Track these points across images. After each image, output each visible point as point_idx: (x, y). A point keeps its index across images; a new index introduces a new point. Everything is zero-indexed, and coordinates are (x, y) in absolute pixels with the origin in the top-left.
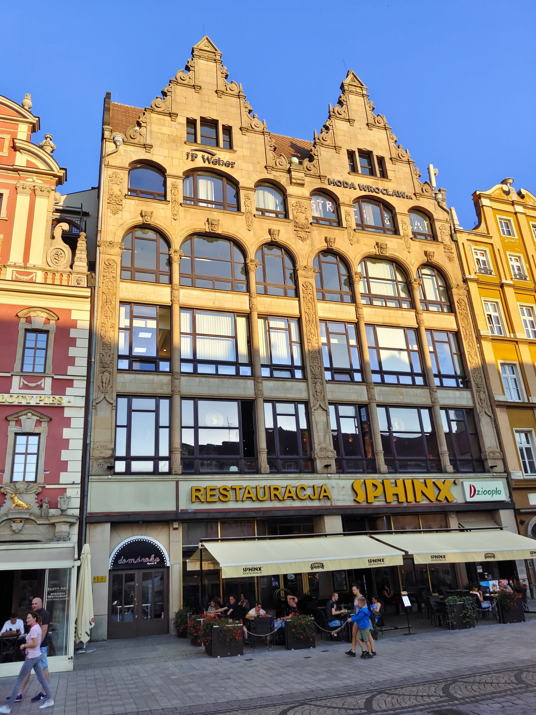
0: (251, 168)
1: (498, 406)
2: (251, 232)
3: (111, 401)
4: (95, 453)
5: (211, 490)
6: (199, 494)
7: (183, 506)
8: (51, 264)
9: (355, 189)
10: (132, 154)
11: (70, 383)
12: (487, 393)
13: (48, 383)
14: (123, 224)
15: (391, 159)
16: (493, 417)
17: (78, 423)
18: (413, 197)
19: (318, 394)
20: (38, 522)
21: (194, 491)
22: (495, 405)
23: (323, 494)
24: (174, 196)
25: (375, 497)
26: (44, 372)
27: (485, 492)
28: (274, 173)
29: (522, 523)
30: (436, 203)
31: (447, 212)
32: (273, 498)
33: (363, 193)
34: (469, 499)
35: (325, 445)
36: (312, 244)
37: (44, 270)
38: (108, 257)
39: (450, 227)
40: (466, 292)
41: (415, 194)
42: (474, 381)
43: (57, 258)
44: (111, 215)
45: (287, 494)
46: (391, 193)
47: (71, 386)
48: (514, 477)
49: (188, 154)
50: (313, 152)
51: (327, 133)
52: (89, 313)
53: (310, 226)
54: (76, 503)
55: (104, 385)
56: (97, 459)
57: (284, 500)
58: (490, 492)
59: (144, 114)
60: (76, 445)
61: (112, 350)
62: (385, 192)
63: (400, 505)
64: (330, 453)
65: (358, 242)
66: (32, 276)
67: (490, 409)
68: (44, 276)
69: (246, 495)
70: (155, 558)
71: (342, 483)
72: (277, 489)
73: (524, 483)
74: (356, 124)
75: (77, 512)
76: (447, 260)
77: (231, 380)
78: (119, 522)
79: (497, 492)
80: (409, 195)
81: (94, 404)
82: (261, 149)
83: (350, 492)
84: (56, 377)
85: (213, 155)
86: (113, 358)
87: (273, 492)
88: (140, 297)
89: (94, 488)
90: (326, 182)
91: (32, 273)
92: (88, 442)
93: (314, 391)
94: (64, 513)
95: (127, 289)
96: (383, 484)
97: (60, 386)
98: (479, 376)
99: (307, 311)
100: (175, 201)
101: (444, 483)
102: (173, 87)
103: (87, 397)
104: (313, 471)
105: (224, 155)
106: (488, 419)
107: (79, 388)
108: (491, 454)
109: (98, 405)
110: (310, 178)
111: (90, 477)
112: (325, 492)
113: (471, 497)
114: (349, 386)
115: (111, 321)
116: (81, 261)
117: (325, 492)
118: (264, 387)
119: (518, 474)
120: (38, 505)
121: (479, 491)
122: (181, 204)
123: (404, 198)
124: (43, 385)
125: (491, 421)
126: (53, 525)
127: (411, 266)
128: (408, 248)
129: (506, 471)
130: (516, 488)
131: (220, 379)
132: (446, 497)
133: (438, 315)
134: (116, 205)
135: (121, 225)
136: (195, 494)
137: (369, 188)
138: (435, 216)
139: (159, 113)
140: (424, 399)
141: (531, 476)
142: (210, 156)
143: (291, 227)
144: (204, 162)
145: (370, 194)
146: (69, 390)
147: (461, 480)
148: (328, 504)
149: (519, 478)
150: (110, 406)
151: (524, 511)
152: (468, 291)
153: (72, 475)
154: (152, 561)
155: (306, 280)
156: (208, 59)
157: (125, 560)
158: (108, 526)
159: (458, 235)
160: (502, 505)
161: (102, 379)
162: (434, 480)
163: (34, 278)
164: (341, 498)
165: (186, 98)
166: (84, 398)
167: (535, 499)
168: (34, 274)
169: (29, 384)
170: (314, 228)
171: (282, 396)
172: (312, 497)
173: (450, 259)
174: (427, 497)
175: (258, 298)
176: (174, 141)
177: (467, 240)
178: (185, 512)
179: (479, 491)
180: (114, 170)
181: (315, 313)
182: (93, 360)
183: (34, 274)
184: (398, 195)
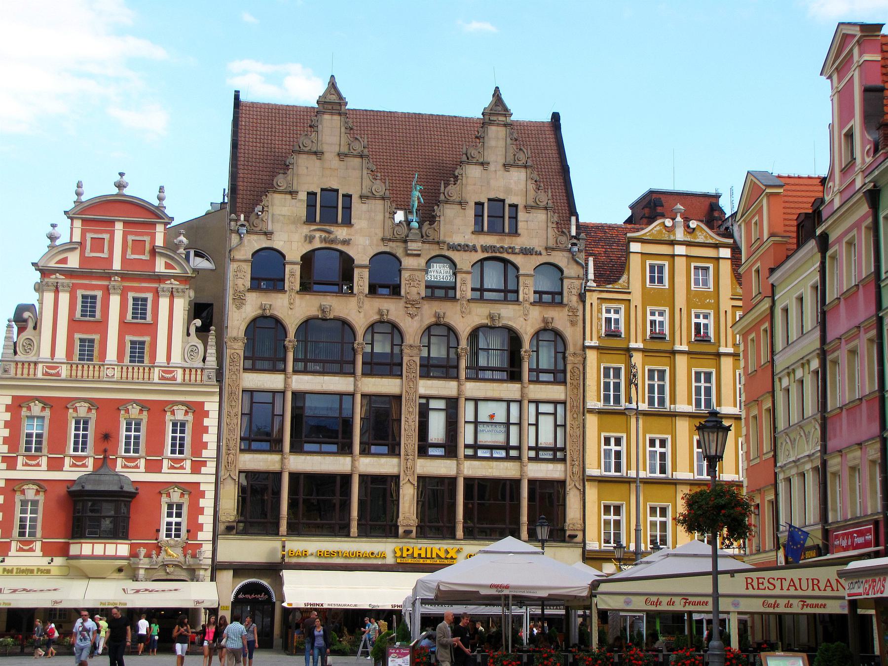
1: (588, 480)
2: (362, 315)
4: (222, 518)
11: (204, 463)
13: (188, 464)
17: (210, 495)
18: (544, 252)
22: (585, 479)
28: (391, 244)
31: (583, 267)
33: (486, 255)
36: (421, 320)
38: (233, 351)
40: (582, 360)
44: (235, 309)
46: (517, 251)
47: (205, 466)
49: (306, 237)
54: (209, 554)
56: (224, 522)
60: (209, 512)
62: (510, 251)
65: (470, 313)
75: (209, 562)
76: (569, 324)
78: (239, 569)
80: (538, 249)
85: (329, 232)
89: (221, 543)
90: (446, 247)
91: (173, 371)
97: (197, 468)
104: (396, 536)
106: (577, 492)
107: (211, 467)
115: (235, 410)
127: (524, 335)
134: (240, 301)
137: (493, 248)
139: (280, 192)
142: (327, 235)
145: (494, 255)
146: (204, 470)
152: (585, 359)
153: (206, 535)
154: (262, 597)
158: (231, 573)
170: (425, 302)
173: (573, 323)
176: (294, 223)
180: (240, 264)
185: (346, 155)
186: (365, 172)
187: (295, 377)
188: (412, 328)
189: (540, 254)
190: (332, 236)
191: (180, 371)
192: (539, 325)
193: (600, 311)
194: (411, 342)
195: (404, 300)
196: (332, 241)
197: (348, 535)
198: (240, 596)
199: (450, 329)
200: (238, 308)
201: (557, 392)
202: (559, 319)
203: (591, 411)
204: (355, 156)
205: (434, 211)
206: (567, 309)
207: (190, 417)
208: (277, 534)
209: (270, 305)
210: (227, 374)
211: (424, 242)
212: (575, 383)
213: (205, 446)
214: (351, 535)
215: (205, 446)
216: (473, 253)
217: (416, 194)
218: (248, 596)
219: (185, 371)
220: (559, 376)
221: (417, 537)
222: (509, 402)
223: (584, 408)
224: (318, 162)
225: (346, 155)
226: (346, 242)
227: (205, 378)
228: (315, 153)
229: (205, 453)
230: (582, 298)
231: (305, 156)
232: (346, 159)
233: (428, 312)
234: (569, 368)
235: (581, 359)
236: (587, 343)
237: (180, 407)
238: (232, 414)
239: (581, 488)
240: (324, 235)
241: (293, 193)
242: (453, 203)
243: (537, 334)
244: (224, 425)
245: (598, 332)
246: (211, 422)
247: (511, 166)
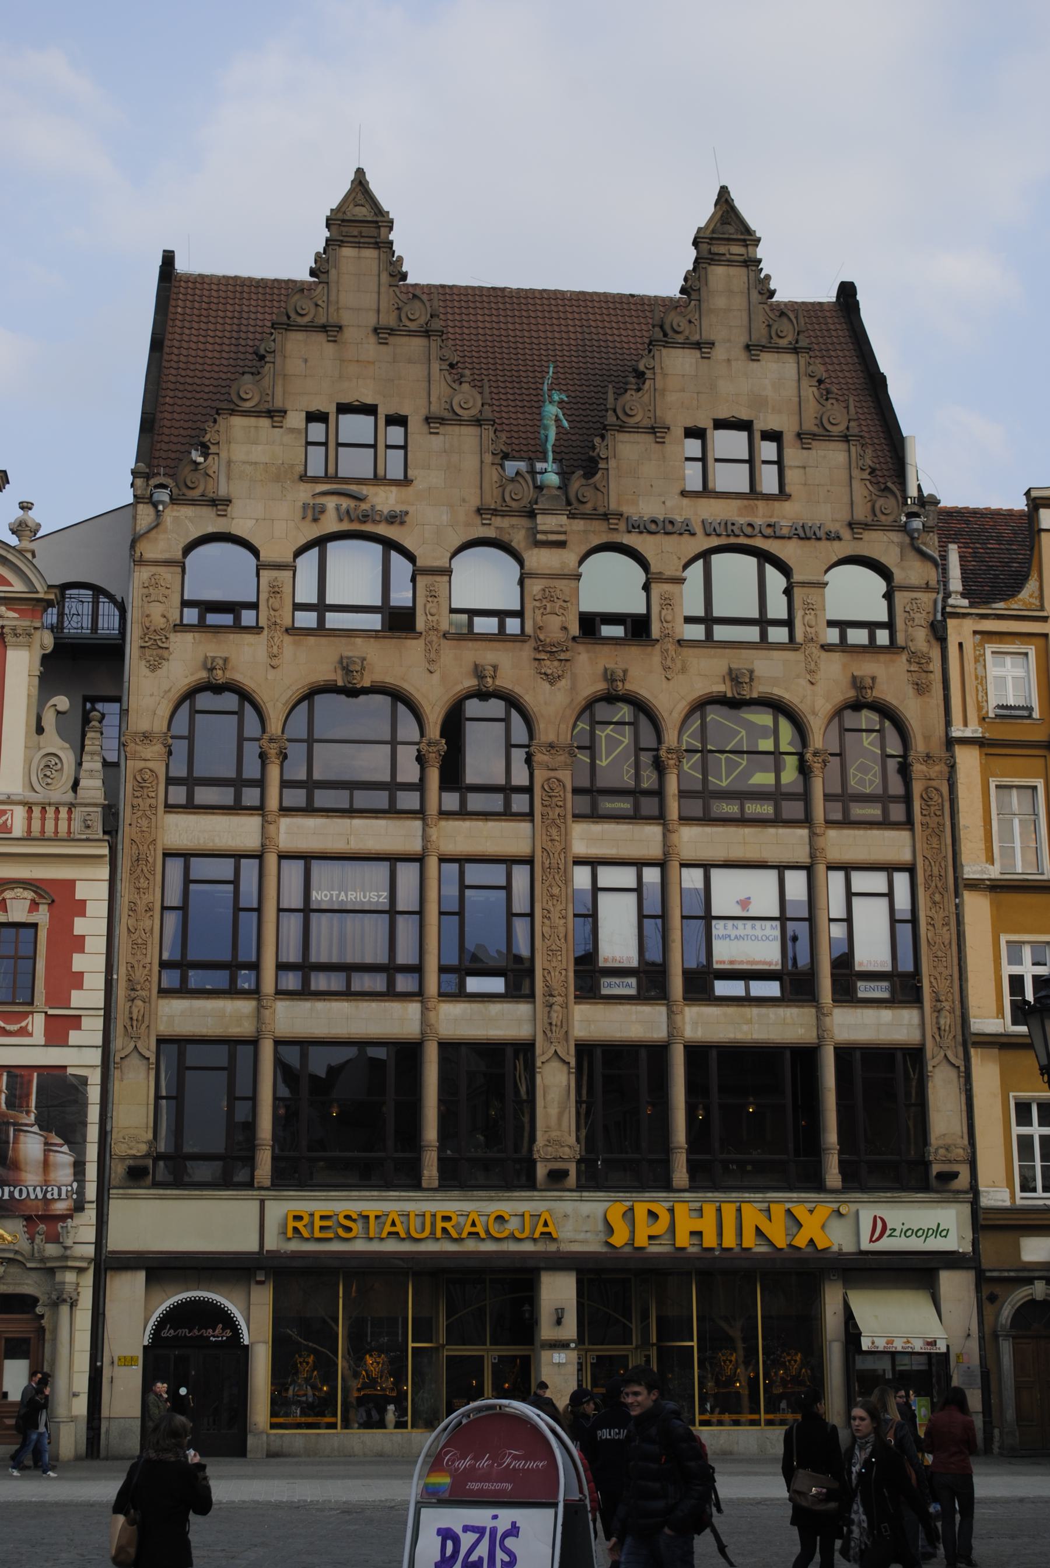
0: (444, 517)
1: (976, 1044)
2: (436, 676)
3: (147, 1054)
4: (119, 1148)
5: (322, 1218)
6: (299, 1225)
7: (272, 1243)
8: (37, 787)
9: (693, 534)
10: (190, 525)
11: (75, 1022)
12: (958, 1013)
13: (37, 1024)
14: (169, 690)
15: (799, 436)
16: (962, 1069)
18: (846, 534)
19: (554, 1028)
20: (29, 1265)
21: (290, 1218)
22: (971, 1041)
23: (540, 1229)
24: (272, 613)
25: (650, 1237)
26: (32, 1003)
27: (906, 1233)
28: (498, 521)
29: (993, 1298)
30: (907, 540)
31: (936, 564)
32: (439, 1234)
33: (715, 542)
34: (866, 1245)
35: (558, 1133)
36: (573, 688)
37: (24, 804)
38: (142, 764)
39: (935, 602)
40: (946, 769)
41: (851, 525)
42: (932, 986)
43: (48, 773)
44: (145, 671)
45: (468, 1229)
46: (785, 532)
47: (78, 1027)
48: (985, 1201)
49: (305, 506)
50: (597, 450)
51: (638, 390)
52: (106, 885)
53: (570, 644)
55: (135, 1023)
56: (122, 1159)
57: (462, 1239)
58: (920, 1233)
59: (215, 421)
61: (149, 956)
63: (708, 1255)
64: (567, 1149)
65: (684, 670)
66: (4, 818)
67: (960, 1049)
68: (26, 815)
69: (388, 1228)
70: (223, 1329)
71: (586, 1208)
72: (447, 1218)
73: (1007, 1216)
74: (719, 353)
75: (90, 1251)
76: (910, 691)
77: (374, 1005)
78: (161, 1269)
79: (939, 1232)
80: (833, 527)
81: (117, 1059)
82: (470, 463)
83: (601, 1227)
84: (51, 1012)
86: (150, 970)
87: (440, 1224)
88: (201, 841)
89: (118, 1209)
90: (622, 526)
92: (108, 1128)
93: (546, 1021)
94: (69, 1252)
95: (177, 826)
96: (671, 1211)
97: (59, 1030)
98: (949, 972)
99: (548, 846)
100: (275, 624)
101: (811, 1211)
102: (279, 338)
103: (106, 1047)
104: (531, 1184)
105: (385, 499)
106: (952, 1074)
107: (91, 1031)
108: (942, 1151)
109: (126, 1062)
110: (582, 522)
111: (111, 1191)
112: (546, 1224)
113: (871, 1241)
114: (628, 1007)
115: (147, 898)
116: (92, 777)
117: (546, 1224)
118: (442, 1016)
119: (996, 1195)
120: (27, 1236)
121: (895, 1230)
122: (287, 630)
123: (819, 539)
124: (30, 1028)
125: (959, 1077)
126: (52, 1271)
128: (811, 672)
129: (974, 1189)
130: (985, 1223)
131: (353, 1004)
132: (811, 1240)
133: (869, 832)
134: (157, 650)
135: (166, 692)
136: (291, 1224)
137: (728, 527)
138: (899, 576)
139: (246, 413)
140: (801, 1031)
141: (1041, 1198)
143: (527, 651)
144: (341, 520)
145: (733, 540)
146: (74, 1037)
147: (853, 1207)
148: (552, 1247)
149: (1000, 1204)
150: (145, 1062)
151: (995, 1274)
152: (952, 767)
154: (218, 1335)
155: (552, 774)
156: (359, 245)
157: (172, 1331)
158: (141, 1276)
159: (951, 623)
160: (951, 1260)
161: (131, 1013)
162: (788, 1206)
163: (9, 822)
164: (581, 1236)
165: (306, 361)
166: (100, 1050)
167: (1036, 1250)
168: (9, 813)
169: (8, 1027)
170: (581, 648)
171: (479, 1033)
172: (517, 1235)
173: (921, 689)
174: (769, 1240)
175: (443, 823)
176: (277, 479)
177: (975, 632)
178: (274, 1255)
179: (895, 1230)
180: (153, 569)
181: (565, 849)
182: (115, 977)
183: (9, 813)
184: (805, 534)
185: (392, 331)
186: (436, 366)
187: (285, 822)
188: (553, 704)
189: (839, 538)
190: (364, 506)
191: (20, 812)
192: (844, 693)
193: (980, 659)
194: (551, 737)
195: (532, 643)
196: (365, 518)
197: (417, 1186)
198: (168, 1333)
199: (642, 707)
200: (153, 668)
201: (895, 845)
202: (891, 681)
203: (974, 885)
204: (412, 333)
205: (593, 448)
206: (904, 657)
207: (42, 917)
208: (249, 1185)
209: (226, 660)
210: (126, 815)
211: (572, 516)
212: (933, 822)
213: (77, 980)
214: (425, 1184)
215: (77, 980)
216: (686, 537)
217: (552, 410)
218: (184, 1332)
219: (30, 810)
220: (897, 808)
221: (580, 1188)
222: (781, 868)
223: (956, 879)
224: (330, 349)
225: (392, 331)
226: (395, 519)
227: (77, 825)
228: (324, 328)
229: (78, 998)
230: (938, 633)
231: (300, 336)
232: (392, 340)
233: (588, 671)
234: (917, 788)
235: (940, 768)
236: (957, 732)
237: (19, 892)
238: (141, 907)
239: (960, 1063)
240: (345, 503)
241: (275, 415)
242: (637, 429)
243: (838, 713)
244: (121, 930)
245: (980, 708)
246: (91, 927)
247: (763, 348)
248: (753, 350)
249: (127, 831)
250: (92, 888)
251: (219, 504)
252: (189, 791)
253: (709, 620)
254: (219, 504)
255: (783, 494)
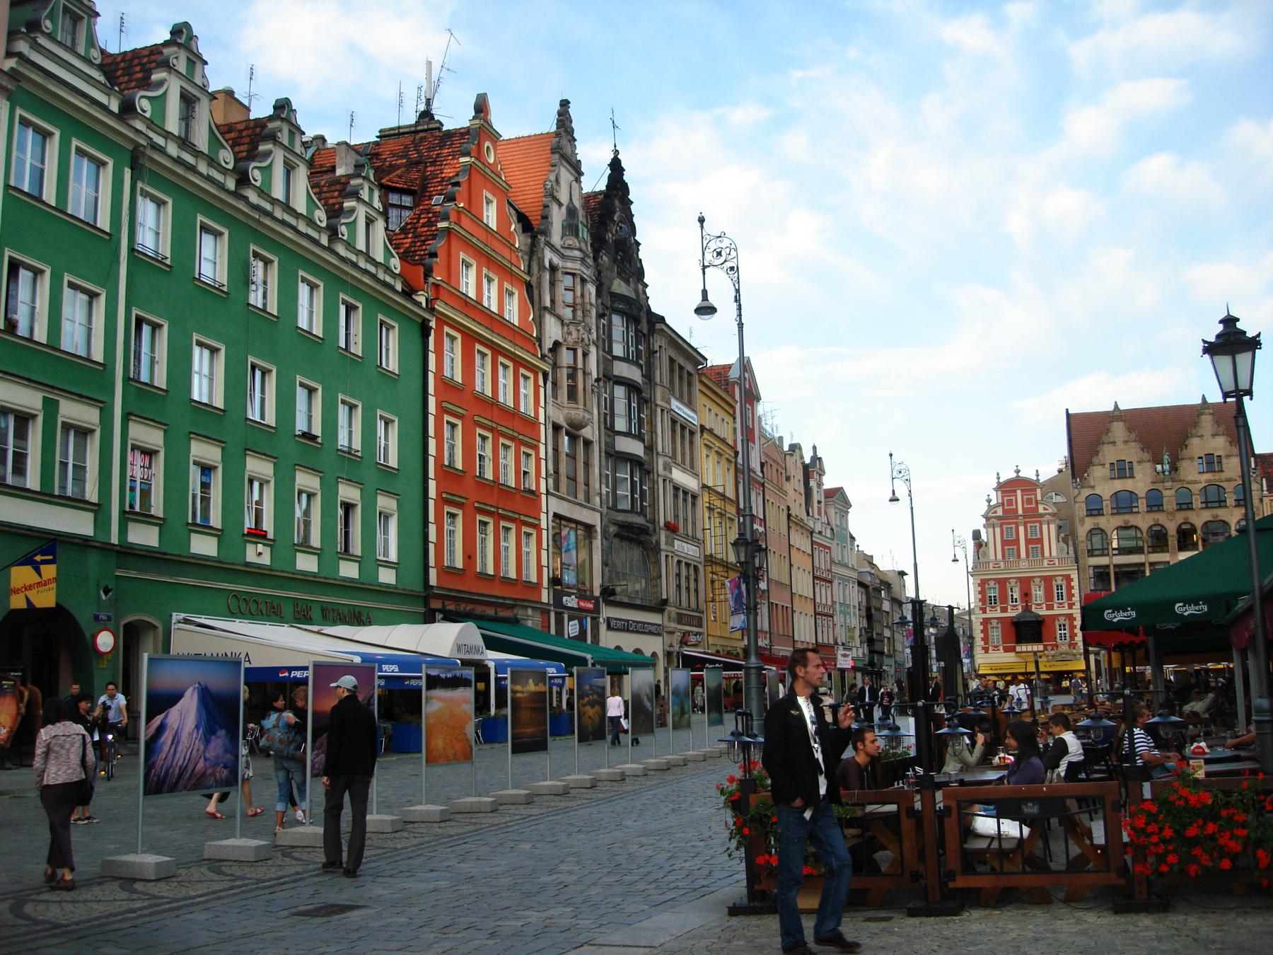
97: (1070, 606)
134: (1082, 521)
246: (1075, 584)
248: (1214, 435)
249: (1081, 562)
250: (1074, 575)
251: (1093, 487)
252: (1091, 553)
253: (1206, 502)
254: (1093, 487)
255: (1222, 471)
